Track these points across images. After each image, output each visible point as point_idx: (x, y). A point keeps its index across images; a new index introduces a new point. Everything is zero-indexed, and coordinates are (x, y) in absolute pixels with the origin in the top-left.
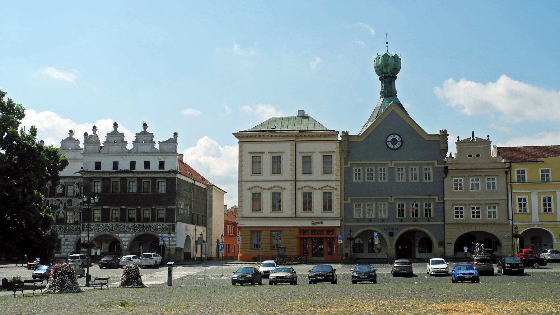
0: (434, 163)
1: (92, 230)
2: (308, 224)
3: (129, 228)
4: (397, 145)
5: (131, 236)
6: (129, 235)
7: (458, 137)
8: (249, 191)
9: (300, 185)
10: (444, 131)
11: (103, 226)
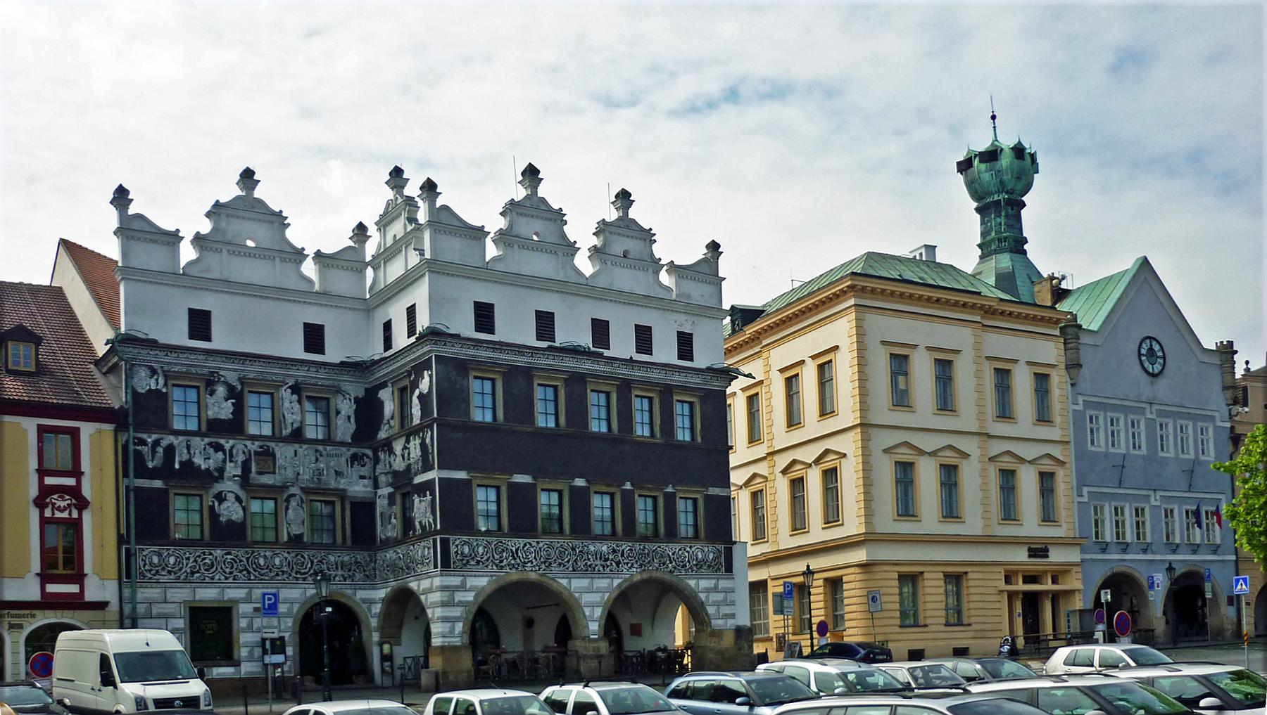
0: (1214, 416)
1: (478, 562)
3: (601, 559)
4: (1157, 365)
5: (608, 588)
6: (603, 583)
7: (1247, 363)
8: (888, 455)
10: (1225, 343)
11: (517, 550)
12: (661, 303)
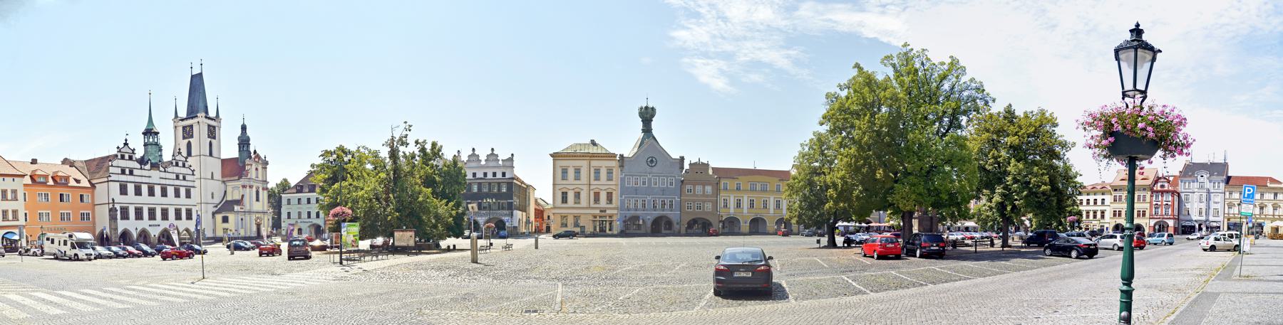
2: (597, 212)
9: (592, 187)
12: (499, 167)
